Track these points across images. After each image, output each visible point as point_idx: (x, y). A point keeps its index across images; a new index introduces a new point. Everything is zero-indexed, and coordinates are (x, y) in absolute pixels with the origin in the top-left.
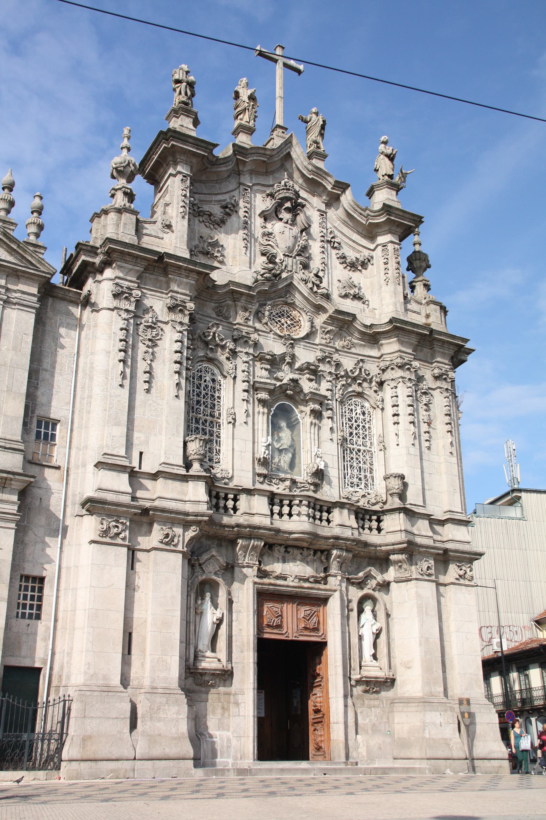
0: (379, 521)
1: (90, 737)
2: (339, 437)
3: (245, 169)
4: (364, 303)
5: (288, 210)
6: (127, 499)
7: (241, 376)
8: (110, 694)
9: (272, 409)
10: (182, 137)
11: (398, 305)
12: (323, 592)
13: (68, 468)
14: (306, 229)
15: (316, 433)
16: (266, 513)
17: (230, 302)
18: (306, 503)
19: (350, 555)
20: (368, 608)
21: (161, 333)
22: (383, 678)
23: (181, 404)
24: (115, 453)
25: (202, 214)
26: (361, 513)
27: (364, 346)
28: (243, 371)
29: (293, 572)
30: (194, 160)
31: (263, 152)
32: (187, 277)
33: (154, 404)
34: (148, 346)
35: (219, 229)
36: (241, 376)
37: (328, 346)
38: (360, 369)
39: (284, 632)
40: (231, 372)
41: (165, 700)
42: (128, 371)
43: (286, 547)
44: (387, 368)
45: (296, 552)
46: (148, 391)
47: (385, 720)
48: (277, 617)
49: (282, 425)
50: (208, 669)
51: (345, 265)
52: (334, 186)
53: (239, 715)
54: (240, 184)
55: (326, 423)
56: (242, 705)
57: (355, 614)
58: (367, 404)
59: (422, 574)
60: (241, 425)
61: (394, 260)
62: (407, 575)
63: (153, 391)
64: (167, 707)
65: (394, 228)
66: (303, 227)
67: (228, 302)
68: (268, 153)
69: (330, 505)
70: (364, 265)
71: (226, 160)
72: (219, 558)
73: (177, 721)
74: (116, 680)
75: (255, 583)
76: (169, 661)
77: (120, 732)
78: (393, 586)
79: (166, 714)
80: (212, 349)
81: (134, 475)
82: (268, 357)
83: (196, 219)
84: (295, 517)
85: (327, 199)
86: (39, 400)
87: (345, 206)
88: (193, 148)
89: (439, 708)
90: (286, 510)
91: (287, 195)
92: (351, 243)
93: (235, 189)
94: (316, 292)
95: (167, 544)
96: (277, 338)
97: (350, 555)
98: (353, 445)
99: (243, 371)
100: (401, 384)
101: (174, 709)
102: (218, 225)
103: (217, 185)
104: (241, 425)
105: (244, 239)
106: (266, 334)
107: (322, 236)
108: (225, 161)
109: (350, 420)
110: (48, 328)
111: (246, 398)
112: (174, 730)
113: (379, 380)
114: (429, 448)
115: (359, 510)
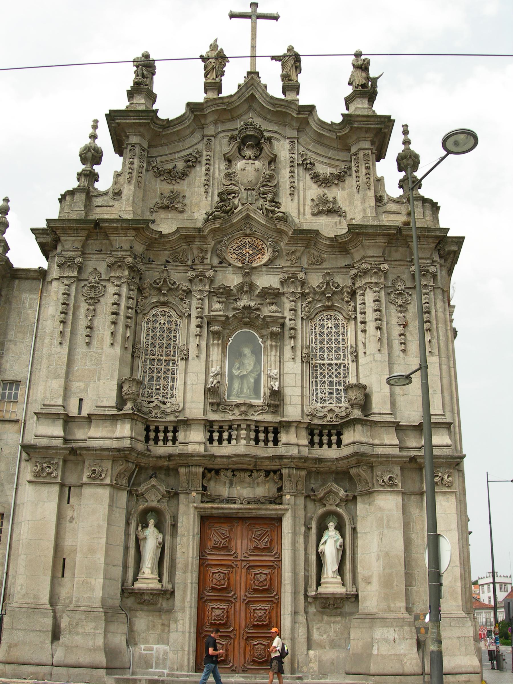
0: (339, 434)
1: (16, 645)
2: (304, 355)
3: (208, 122)
4: (340, 216)
5: (251, 147)
6: (59, 442)
7: (194, 313)
8: (36, 610)
9: (230, 339)
10: (123, 114)
11: (368, 210)
12: (273, 512)
13: (25, 420)
14: (273, 160)
15: (278, 354)
16: (201, 441)
17: (186, 247)
18: (245, 426)
19: (304, 473)
20: (331, 525)
21: (103, 289)
22: (341, 594)
23: (118, 350)
24: (53, 403)
25: (162, 173)
26: (317, 429)
27: (336, 258)
28: (197, 308)
29: (242, 494)
30: (142, 129)
31: (220, 101)
32: (126, 235)
33: (95, 355)
34: (90, 304)
35: (182, 182)
36: (194, 313)
37: (292, 267)
38: (328, 284)
39: (232, 553)
40: (184, 311)
41: (83, 617)
42: (68, 330)
43: (233, 471)
44: (356, 276)
45: (242, 474)
46: (88, 344)
47: (346, 635)
48: (223, 539)
49: (246, 352)
50: (144, 590)
51: (319, 183)
52: (299, 111)
53: (177, 631)
54: (203, 136)
55: (289, 343)
56: (181, 622)
57: (314, 531)
58: (341, 317)
59: (383, 486)
60: (193, 359)
61: (363, 167)
62: (368, 488)
63: (95, 343)
64: (84, 623)
65: (363, 135)
66: (270, 159)
67: (183, 247)
68: (226, 101)
69: (276, 425)
70: (340, 178)
71: (180, 120)
72: (159, 487)
73: (95, 635)
74: (45, 599)
75: (196, 508)
76: (93, 583)
77: (42, 643)
78: (359, 499)
79: (85, 629)
80: (164, 294)
81: (68, 421)
82: (221, 290)
83: (158, 179)
84: (234, 442)
85: (298, 125)
86: (3, 366)
87: (313, 127)
88: (136, 119)
89: (395, 624)
90: (225, 435)
91: (247, 133)
92: (326, 161)
93: (199, 142)
94: (272, 217)
95: (94, 479)
96: (237, 270)
97: (304, 473)
98: (324, 360)
99: (197, 308)
100: (368, 289)
101: (92, 625)
102: (181, 179)
103: (180, 144)
104: (193, 359)
105: (205, 185)
106: (225, 269)
107: (291, 162)
108: (180, 121)
109: (320, 336)
110: (14, 305)
111: (198, 333)
112: (90, 643)
113: (349, 290)
114: (404, 351)
115: (313, 427)
